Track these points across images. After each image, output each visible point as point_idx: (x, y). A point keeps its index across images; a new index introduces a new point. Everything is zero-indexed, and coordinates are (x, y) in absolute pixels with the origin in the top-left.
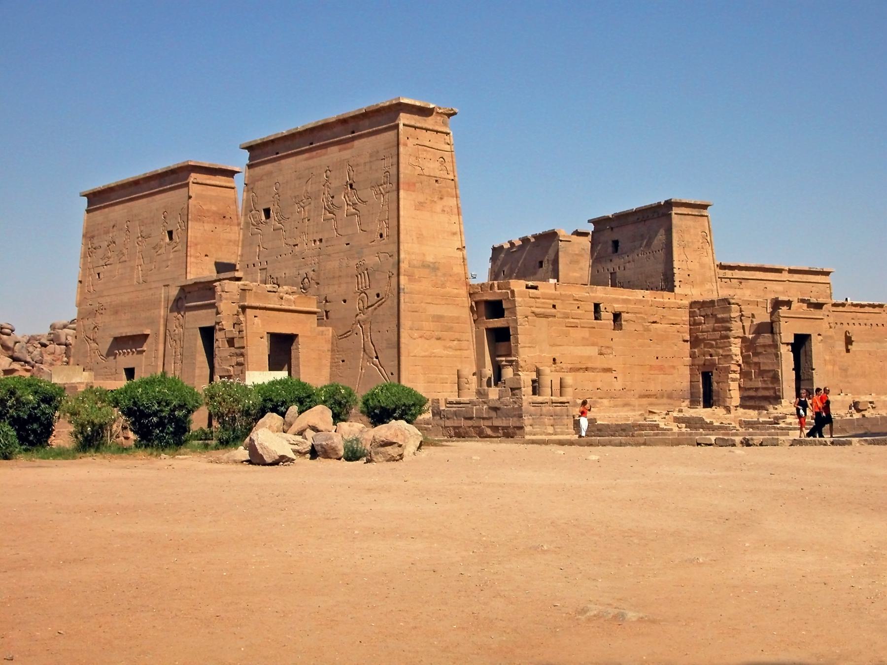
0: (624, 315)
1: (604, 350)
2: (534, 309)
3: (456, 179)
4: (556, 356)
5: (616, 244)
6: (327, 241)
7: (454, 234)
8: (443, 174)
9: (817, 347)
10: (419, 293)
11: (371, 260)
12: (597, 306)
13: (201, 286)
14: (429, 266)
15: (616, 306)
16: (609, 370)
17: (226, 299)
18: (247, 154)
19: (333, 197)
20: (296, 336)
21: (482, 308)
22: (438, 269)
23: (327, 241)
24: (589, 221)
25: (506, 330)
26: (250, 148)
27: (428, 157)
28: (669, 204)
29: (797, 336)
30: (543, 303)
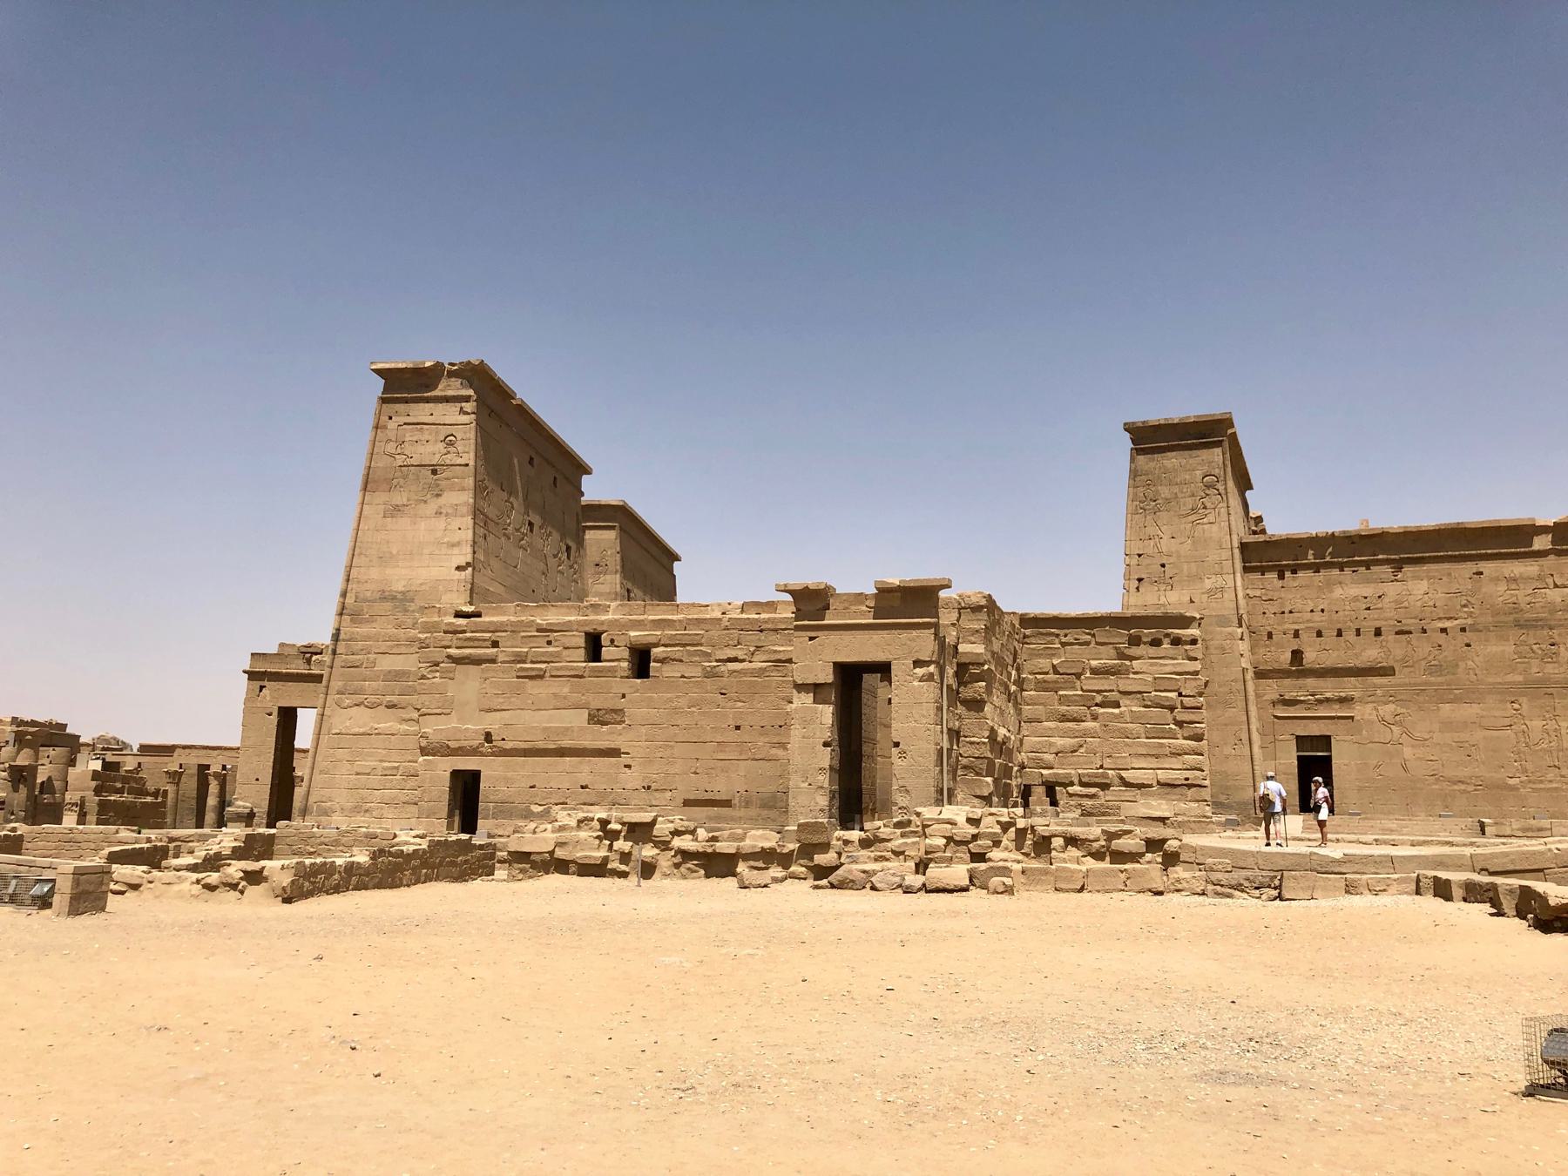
0: (656, 652)
2: (452, 651)
4: (488, 728)
8: (449, 459)
10: (367, 638)
14: (394, 598)
15: (632, 634)
16: (614, 753)
22: (412, 600)
27: (426, 437)
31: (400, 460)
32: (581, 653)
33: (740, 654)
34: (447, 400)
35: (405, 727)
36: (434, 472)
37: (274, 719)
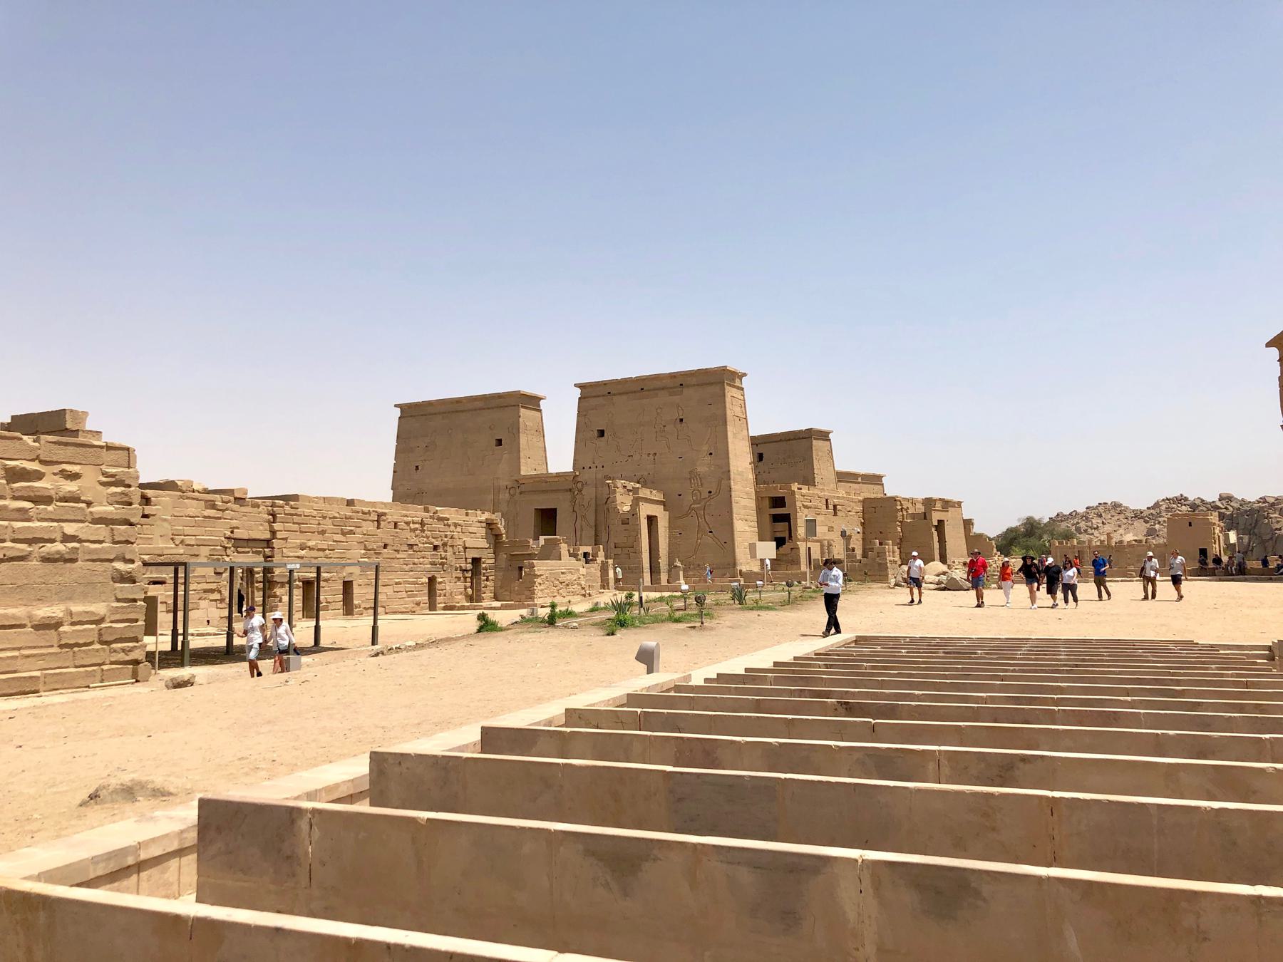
9: (948, 529)
11: (702, 469)
18: (578, 391)
21: (767, 502)
28: (810, 430)
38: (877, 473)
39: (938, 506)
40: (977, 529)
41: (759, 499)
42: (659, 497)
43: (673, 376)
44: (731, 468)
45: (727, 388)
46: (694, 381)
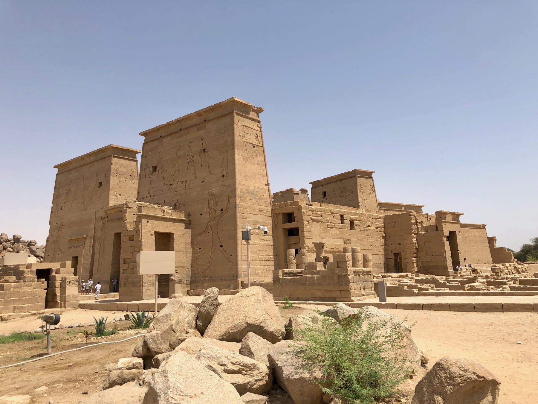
0: (355, 222)
1: (347, 242)
3: (264, 146)
5: (325, 194)
6: (190, 181)
7: (264, 176)
9: (459, 238)
12: (342, 216)
13: (116, 210)
14: (251, 193)
17: (130, 212)
18: (143, 138)
19: (193, 157)
20: (173, 234)
21: (280, 218)
23: (190, 181)
24: (310, 183)
25: (297, 229)
26: (144, 134)
28: (355, 171)
29: (450, 232)
30: (316, 214)
31: (244, 140)
32: (340, 221)
33: (370, 225)
34: (253, 120)
35: (261, 242)
36: (254, 147)
37: (153, 237)
38: (417, 204)
39: (449, 218)
40: (498, 244)
41: (275, 215)
42: (182, 217)
43: (199, 114)
44: (237, 186)
45: (236, 118)
46: (213, 115)
